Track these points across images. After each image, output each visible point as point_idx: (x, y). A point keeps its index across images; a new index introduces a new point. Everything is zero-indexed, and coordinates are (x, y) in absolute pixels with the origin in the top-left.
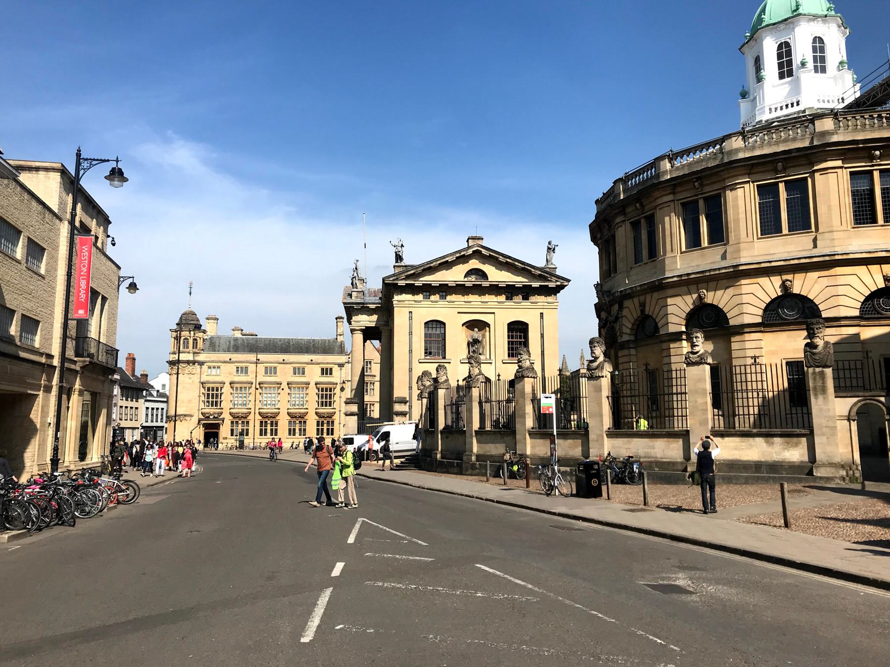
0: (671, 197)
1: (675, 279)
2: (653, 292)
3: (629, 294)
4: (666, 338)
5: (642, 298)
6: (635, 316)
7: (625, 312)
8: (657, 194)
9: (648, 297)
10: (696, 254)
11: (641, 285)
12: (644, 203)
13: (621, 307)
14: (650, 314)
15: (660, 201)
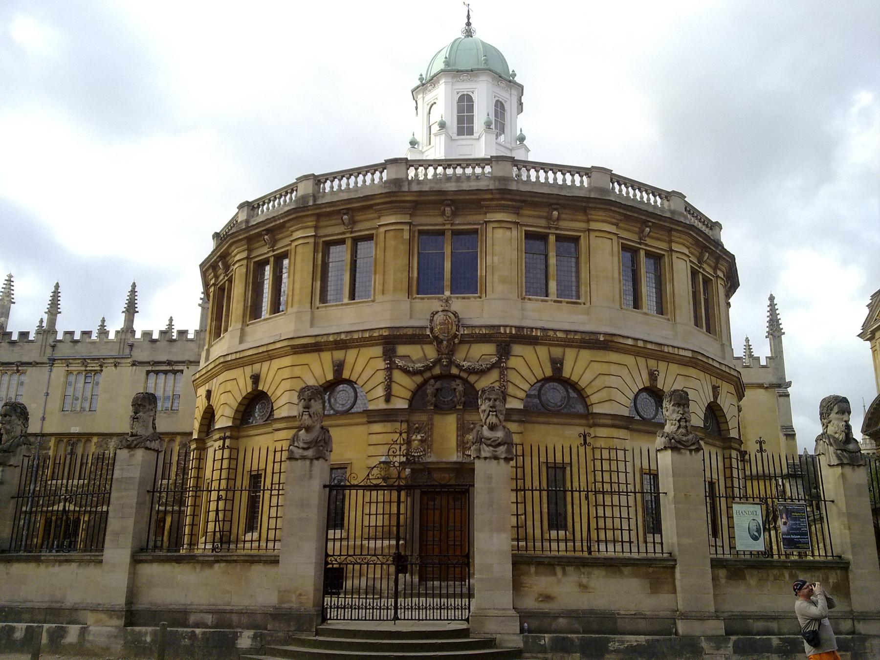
0: (613, 229)
1: (630, 342)
2: (580, 347)
3: (536, 337)
4: (609, 422)
5: (557, 352)
6: (540, 376)
7: (513, 362)
8: (601, 215)
9: (570, 354)
10: (636, 315)
11: (567, 332)
12: (563, 216)
13: (504, 352)
14: (574, 378)
15: (594, 225)
